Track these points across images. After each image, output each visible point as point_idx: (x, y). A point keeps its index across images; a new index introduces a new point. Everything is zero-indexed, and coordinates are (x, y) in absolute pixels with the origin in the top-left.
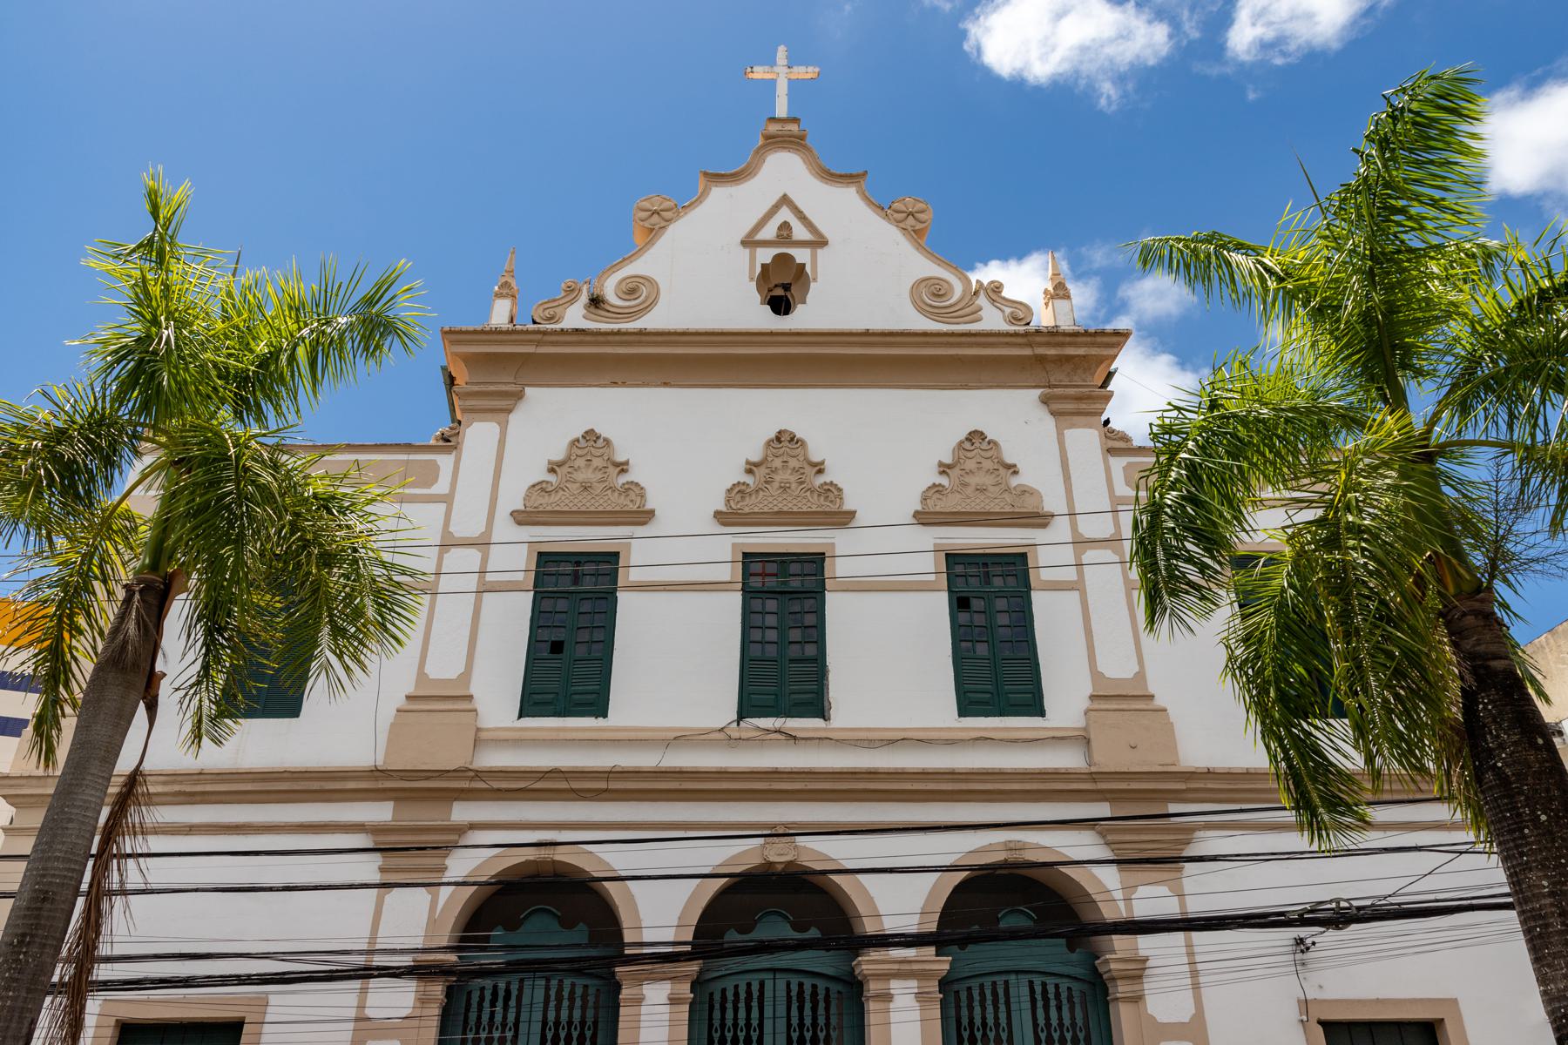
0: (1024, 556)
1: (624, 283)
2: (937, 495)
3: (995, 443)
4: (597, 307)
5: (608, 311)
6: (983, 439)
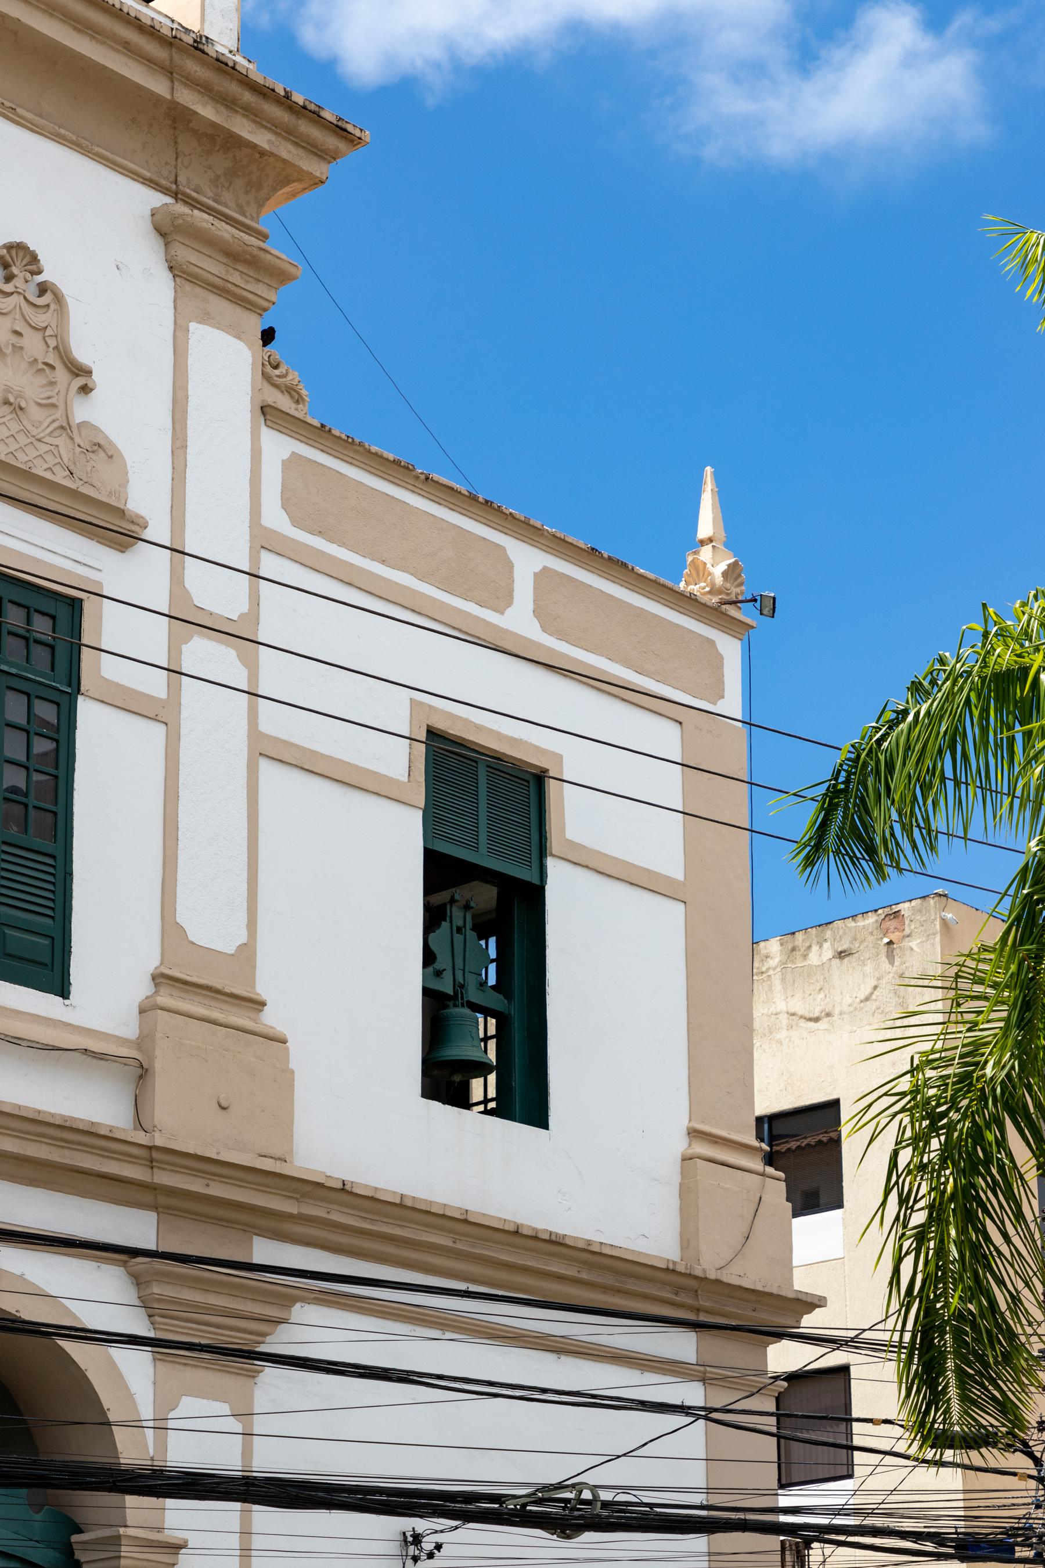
0: (75, 605)
3: (58, 298)
6: (33, 273)
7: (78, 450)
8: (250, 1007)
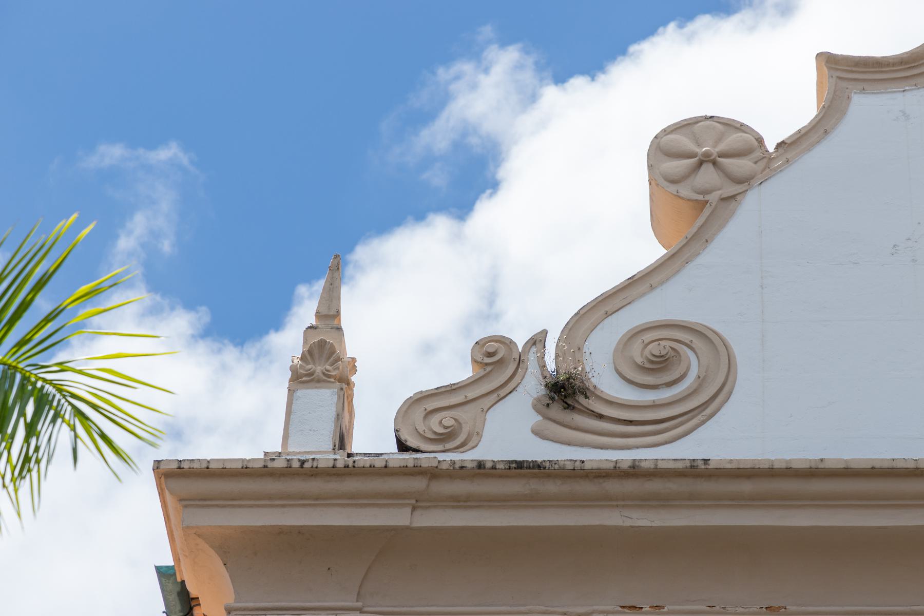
1: (636, 347)
4: (568, 407)
5: (601, 417)
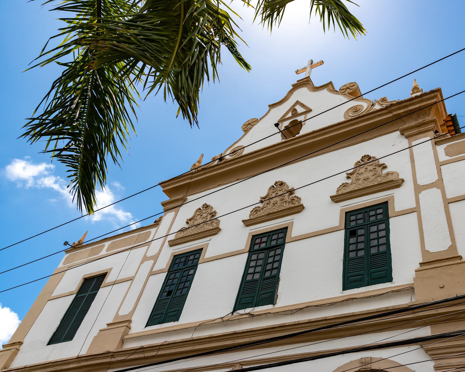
2: (344, 188)
7: (383, 177)
8: (455, 259)
